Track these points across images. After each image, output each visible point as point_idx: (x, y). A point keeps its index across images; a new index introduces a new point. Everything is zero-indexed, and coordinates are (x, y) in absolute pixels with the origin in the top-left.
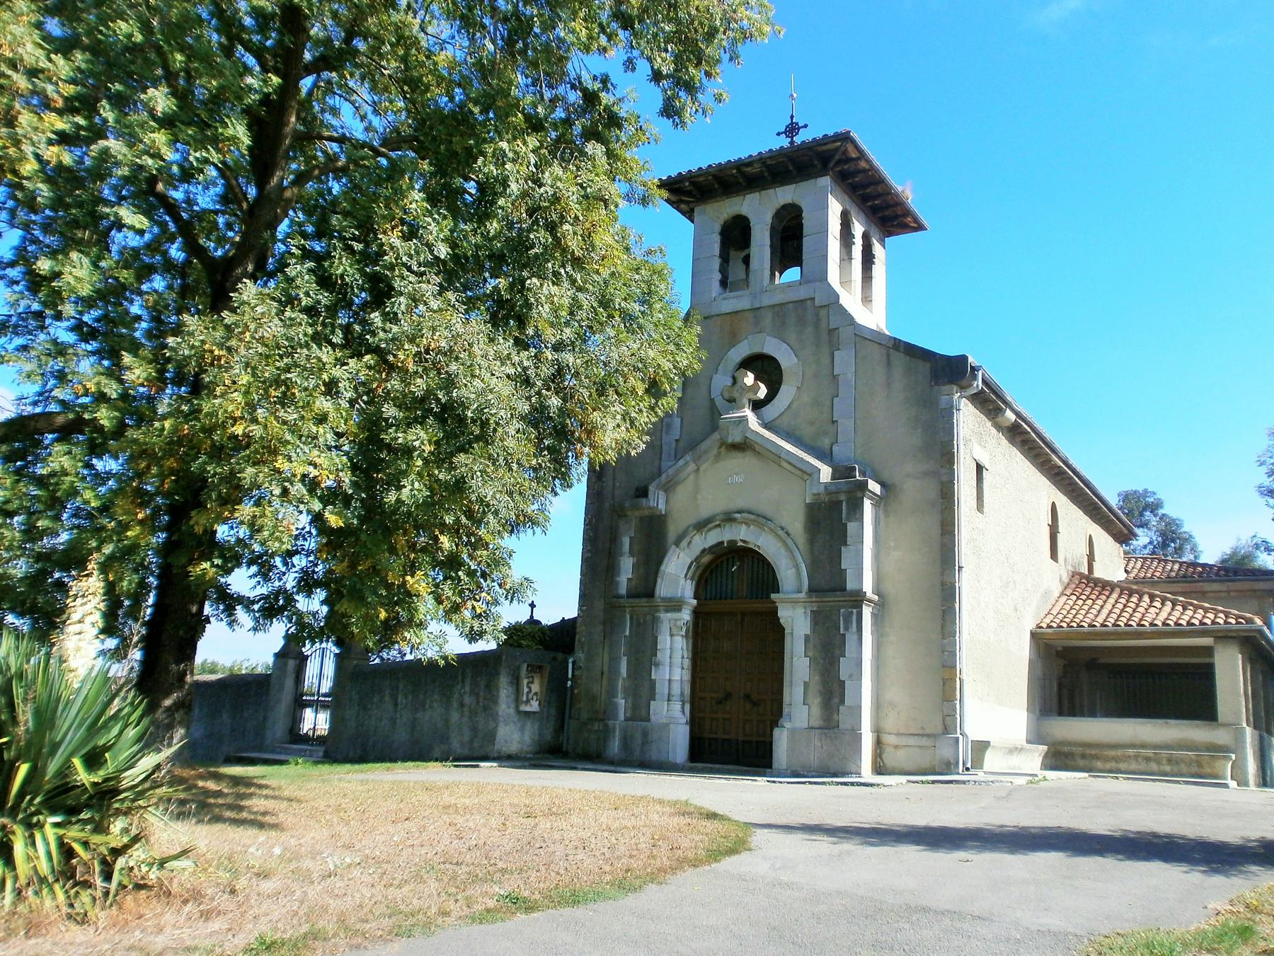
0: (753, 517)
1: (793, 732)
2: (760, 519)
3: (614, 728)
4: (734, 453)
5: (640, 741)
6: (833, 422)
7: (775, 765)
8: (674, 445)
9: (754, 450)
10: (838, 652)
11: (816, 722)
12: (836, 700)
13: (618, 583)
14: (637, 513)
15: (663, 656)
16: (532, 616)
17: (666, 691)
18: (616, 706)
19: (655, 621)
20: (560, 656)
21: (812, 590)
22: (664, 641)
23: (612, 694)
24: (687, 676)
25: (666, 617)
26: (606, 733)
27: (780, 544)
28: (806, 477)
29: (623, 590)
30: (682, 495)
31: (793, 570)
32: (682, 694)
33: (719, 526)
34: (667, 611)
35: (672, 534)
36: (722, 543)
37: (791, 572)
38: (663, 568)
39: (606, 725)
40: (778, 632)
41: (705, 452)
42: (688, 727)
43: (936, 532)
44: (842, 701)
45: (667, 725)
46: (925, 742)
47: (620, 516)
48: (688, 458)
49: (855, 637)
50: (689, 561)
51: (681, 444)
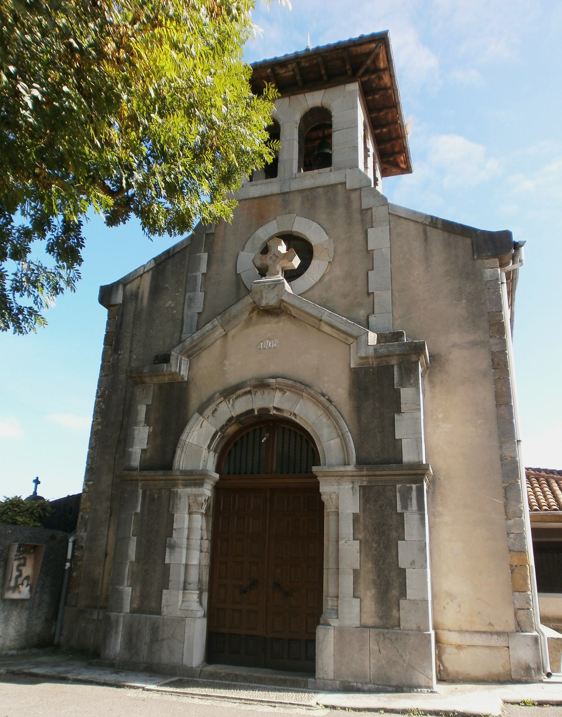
0: (290, 382)
1: (341, 632)
2: (299, 386)
3: (117, 621)
4: (267, 319)
5: (147, 639)
6: (369, 294)
7: (319, 673)
8: (196, 319)
9: (290, 315)
10: (394, 534)
11: (370, 620)
12: (395, 592)
13: (130, 454)
14: (155, 380)
15: (180, 536)
16: (35, 493)
17: (182, 578)
18: (120, 594)
19: (172, 497)
20: (60, 534)
21: (360, 462)
23: (117, 579)
24: (206, 561)
25: (184, 493)
26: (107, 626)
27: (321, 412)
28: (351, 340)
29: (136, 462)
30: (207, 361)
31: (338, 440)
32: (200, 581)
33: (250, 392)
34: (186, 486)
35: (195, 401)
36: (252, 411)
37: (333, 442)
38: (183, 437)
39: (107, 619)
41: (235, 317)
42: (204, 621)
43: (490, 402)
44: (403, 594)
45: (182, 620)
46: (494, 641)
47: (136, 383)
48: (216, 322)
49: (416, 517)
50: (213, 430)
51: (204, 317)
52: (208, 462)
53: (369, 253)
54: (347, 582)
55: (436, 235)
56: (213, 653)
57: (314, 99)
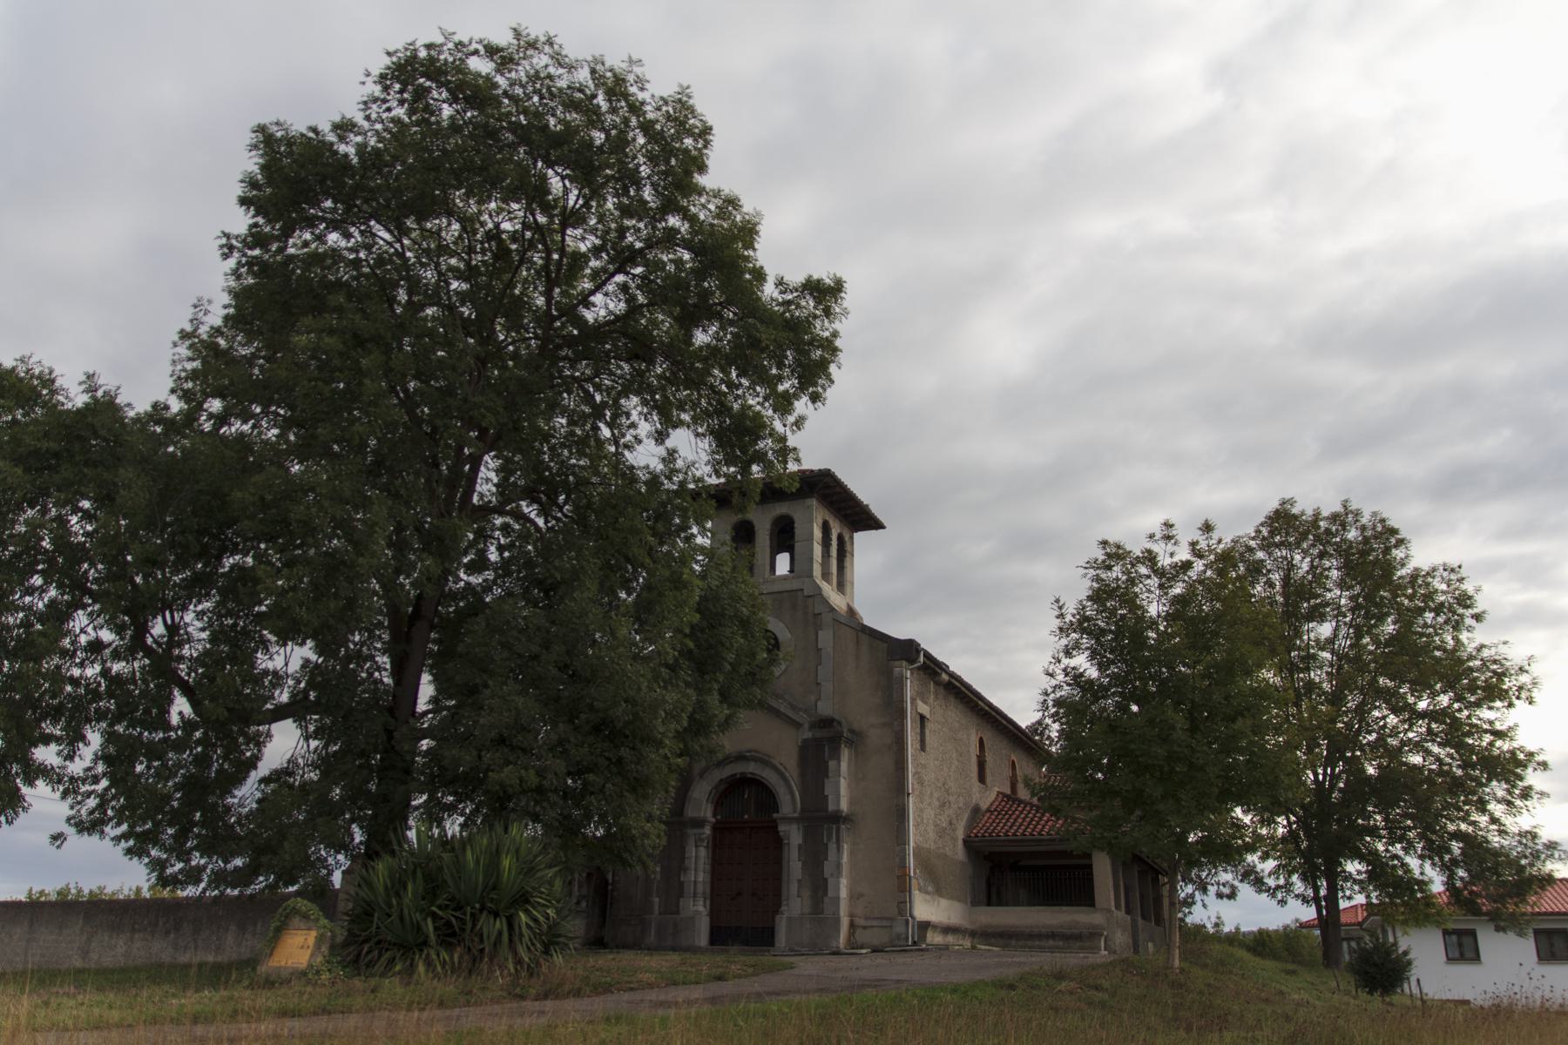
1: (789, 919)
22: (691, 851)
40: (779, 843)
46: (885, 923)
52: (707, 812)
53: (819, 650)
54: (794, 887)
55: (864, 638)
56: (714, 940)
57: (781, 509)
